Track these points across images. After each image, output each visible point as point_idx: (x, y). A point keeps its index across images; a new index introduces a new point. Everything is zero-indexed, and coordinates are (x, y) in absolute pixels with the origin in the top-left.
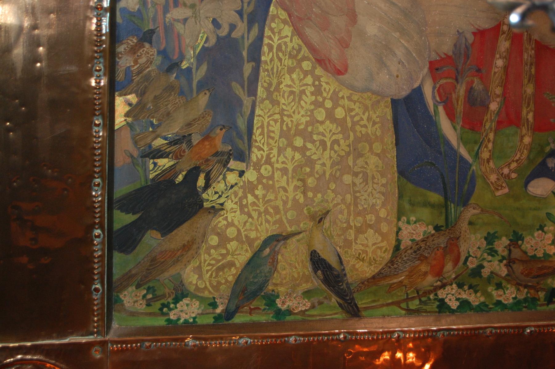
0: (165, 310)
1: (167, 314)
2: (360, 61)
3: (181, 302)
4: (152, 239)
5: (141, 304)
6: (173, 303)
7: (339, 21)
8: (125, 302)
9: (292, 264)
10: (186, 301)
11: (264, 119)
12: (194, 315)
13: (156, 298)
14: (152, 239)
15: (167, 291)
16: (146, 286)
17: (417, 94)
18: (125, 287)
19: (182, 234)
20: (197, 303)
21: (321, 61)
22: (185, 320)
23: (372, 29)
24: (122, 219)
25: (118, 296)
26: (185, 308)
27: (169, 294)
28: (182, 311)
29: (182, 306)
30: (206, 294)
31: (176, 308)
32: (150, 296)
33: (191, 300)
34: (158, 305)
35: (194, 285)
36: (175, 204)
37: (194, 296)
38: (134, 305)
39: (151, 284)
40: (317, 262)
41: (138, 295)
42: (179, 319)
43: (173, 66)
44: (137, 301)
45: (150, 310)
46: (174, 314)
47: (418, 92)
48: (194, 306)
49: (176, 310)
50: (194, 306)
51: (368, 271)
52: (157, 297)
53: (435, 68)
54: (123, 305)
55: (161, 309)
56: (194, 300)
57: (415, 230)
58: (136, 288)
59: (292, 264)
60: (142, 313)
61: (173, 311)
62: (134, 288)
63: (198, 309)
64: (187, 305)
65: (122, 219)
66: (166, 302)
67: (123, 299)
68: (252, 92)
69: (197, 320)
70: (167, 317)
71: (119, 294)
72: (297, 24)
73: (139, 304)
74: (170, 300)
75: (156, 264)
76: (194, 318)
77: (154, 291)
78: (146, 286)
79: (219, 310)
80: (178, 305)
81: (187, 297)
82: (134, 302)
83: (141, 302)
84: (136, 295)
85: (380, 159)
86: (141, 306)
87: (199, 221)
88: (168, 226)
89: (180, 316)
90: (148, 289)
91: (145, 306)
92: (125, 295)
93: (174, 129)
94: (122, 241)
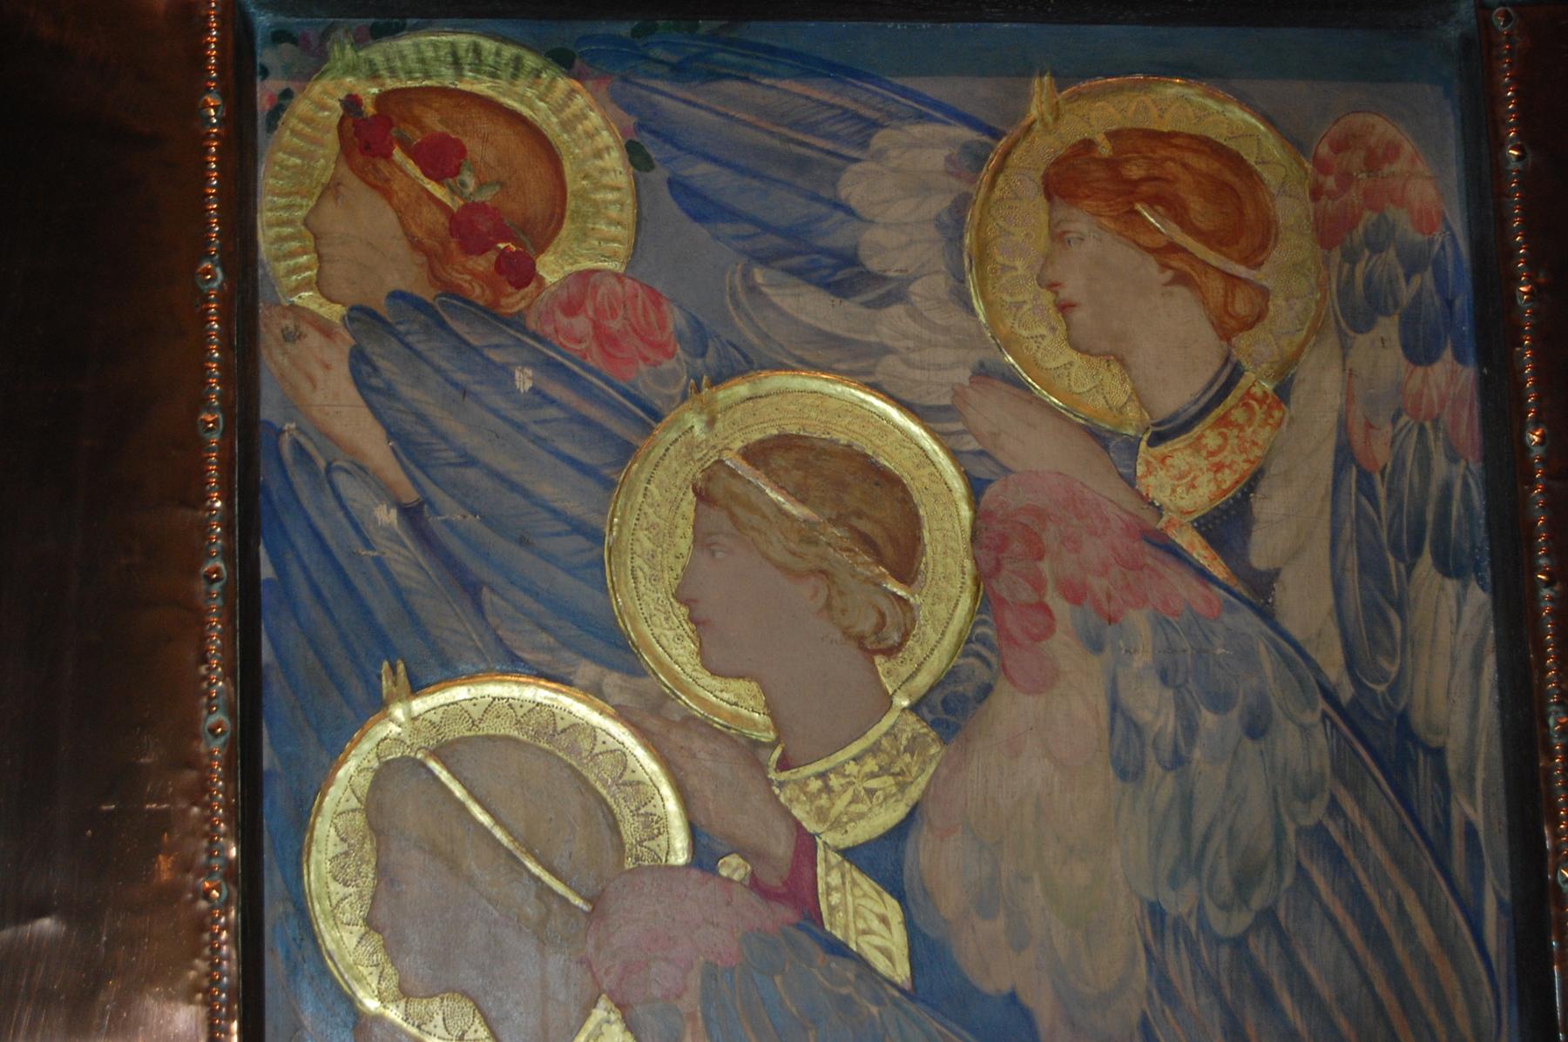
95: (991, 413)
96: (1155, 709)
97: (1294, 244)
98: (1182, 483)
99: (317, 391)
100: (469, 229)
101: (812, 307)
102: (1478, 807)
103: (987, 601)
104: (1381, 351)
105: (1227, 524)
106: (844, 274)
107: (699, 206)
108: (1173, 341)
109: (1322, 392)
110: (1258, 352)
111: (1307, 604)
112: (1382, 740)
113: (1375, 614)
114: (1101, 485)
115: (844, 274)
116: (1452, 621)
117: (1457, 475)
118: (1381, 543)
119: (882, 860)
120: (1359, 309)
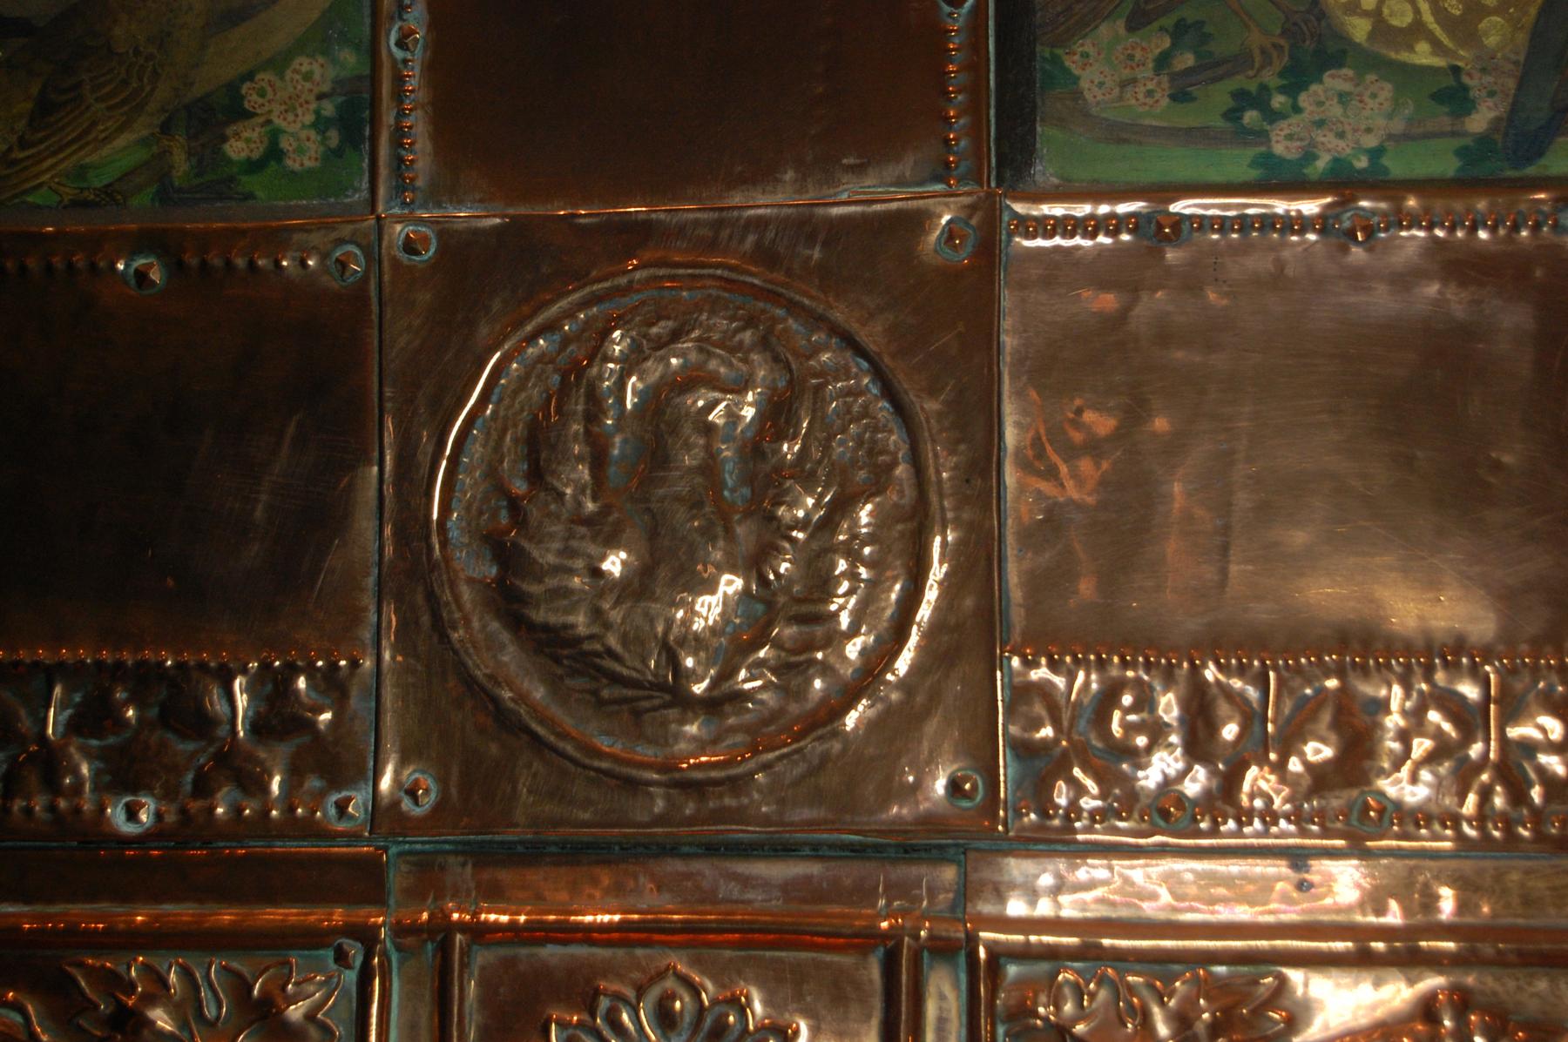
0: (1250, 117)
1: (1262, 136)
3: (1314, 87)
5: (1150, 93)
6: (1282, 90)
8: (1084, 84)
10: (1335, 81)
12: (1371, 142)
13: (1212, 68)
15: (1255, 39)
16: (1169, 21)
18: (1085, 25)
20: (1386, 91)
22: (1336, 160)
25: (1056, 60)
26: (1335, 110)
27: (1263, 51)
28: (1320, 124)
29: (1320, 104)
30: (1422, 55)
31: (1297, 109)
32: (1187, 60)
33: (1358, 80)
34: (1220, 96)
35: (1366, 14)
37: (1370, 62)
38: (1121, 98)
39: (1189, 13)
41: (1138, 54)
42: (1309, 156)
44: (1134, 81)
45: (1187, 117)
46: (1290, 137)
48: (1371, 103)
49: (1294, 119)
50: (1371, 103)
52: (1218, 64)
54: (1078, 95)
55: (1233, 115)
56: (1371, 77)
58: (1132, 28)
60: (1156, 131)
61: (1283, 124)
62: (1120, 25)
63: (1390, 117)
64: (1343, 97)
66: (1253, 87)
67: (1077, 72)
69: (1386, 161)
70: (1263, 149)
71: (1059, 51)
73: (1141, 90)
74: (1270, 78)
76: (1376, 154)
77: (1205, 38)
78: (1169, 21)
79: (1478, 122)
80: (1304, 100)
81: (1341, 65)
82: (1123, 85)
83: (1150, 86)
84: (1131, 57)
86: (1150, 101)
89: (1313, 144)
90: (1179, 32)
91: (1165, 102)
92: (1085, 55)
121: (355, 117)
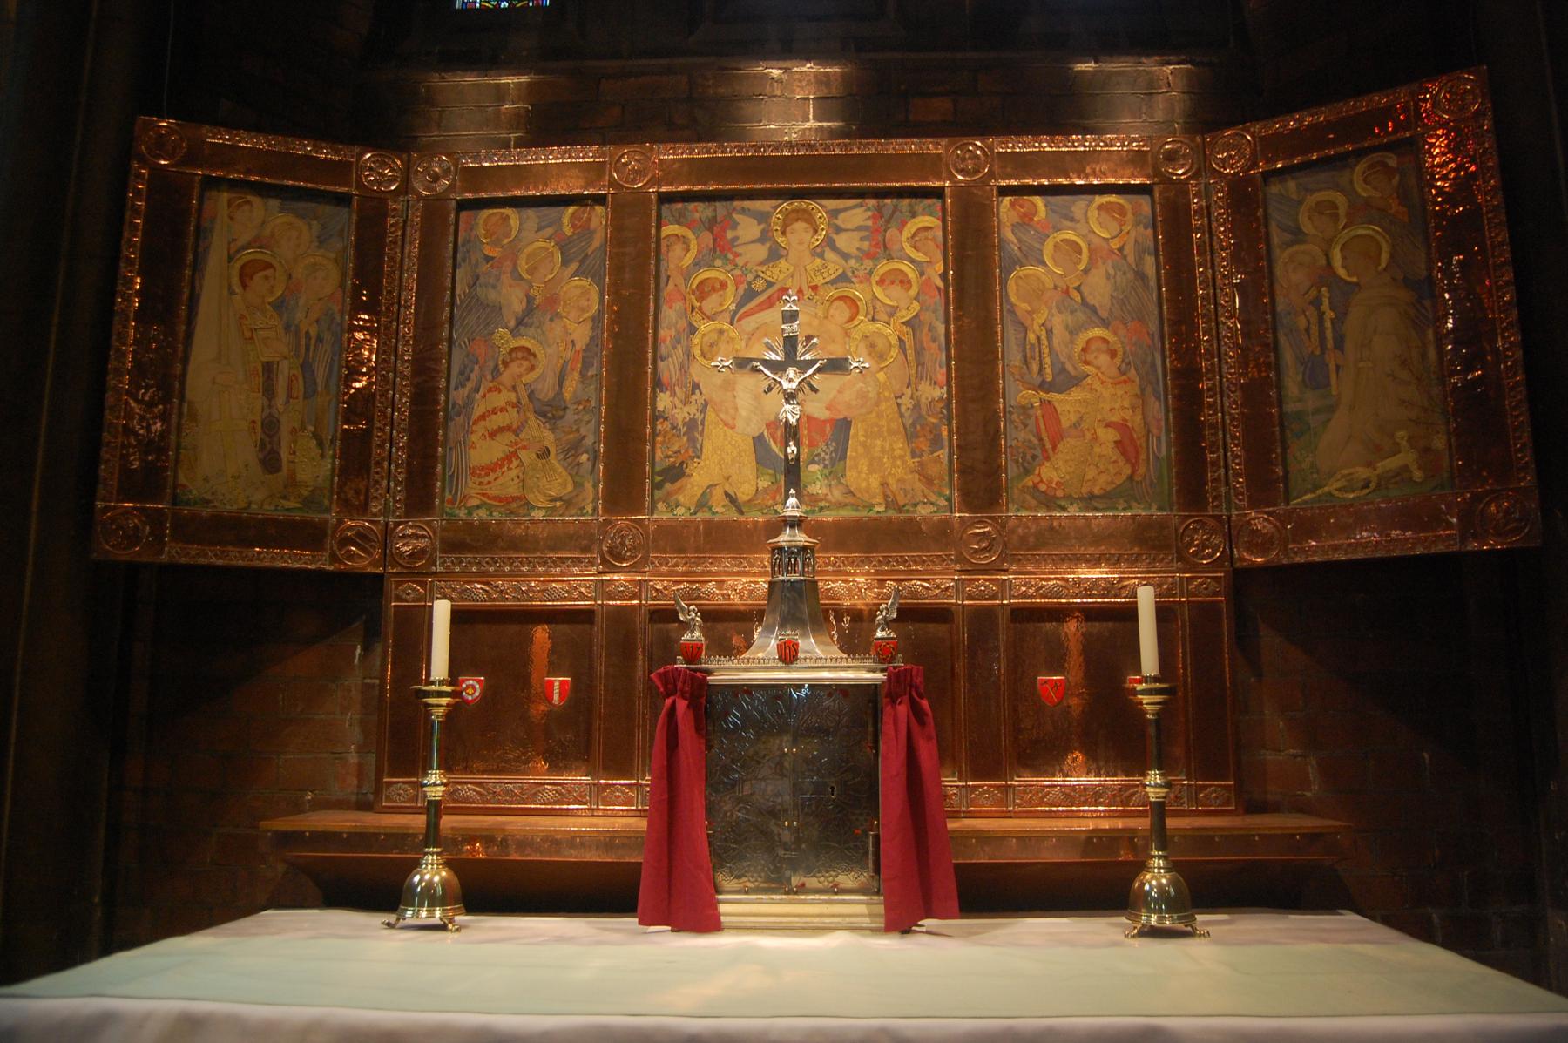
2: (740, 424)
4: (668, 486)
7: (732, 411)
9: (718, 493)
11: (708, 447)
14: (668, 486)
17: (761, 435)
19: (678, 484)
21: (726, 425)
23: (744, 413)
24: (658, 479)
36: (676, 473)
40: (727, 495)
43: (674, 427)
47: (761, 435)
51: (746, 498)
53: (768, 426)
57: (764, 483)
59: (718, 493)
65: (658, 479)
68: (702, 433)
72: (717, 412)
75: (669, 494)
85: (749, 459)
87: (684, 480)
88: (673, 481)
93: (675, 448)
94: (659, 486)
95: (1091, 236)
96: (1111, 271)
97: (1130, 216)
98: (1115, 245)
99: (1009, 234)
100: (1025, 215)
101: (1069, 224)
102: (1153, 283)
103: (1090, 258)
104: (1141, 228)
105: (1121, 249)
106: (1072, 220)
107: (1053, 211)
108: (1114, 227)
109: (1133, 234)
110: (1126, 228)
111: (1131, 259)
112: (1141, 275)
113: (1139, 260)
114: (1104, 244)
115: (1072, 220)
116: (1150, 261)
117: (1151, 244)
118: (1140, 252)
119: (1078, 289)
120: (1137, 223)
121: (595, 509)
